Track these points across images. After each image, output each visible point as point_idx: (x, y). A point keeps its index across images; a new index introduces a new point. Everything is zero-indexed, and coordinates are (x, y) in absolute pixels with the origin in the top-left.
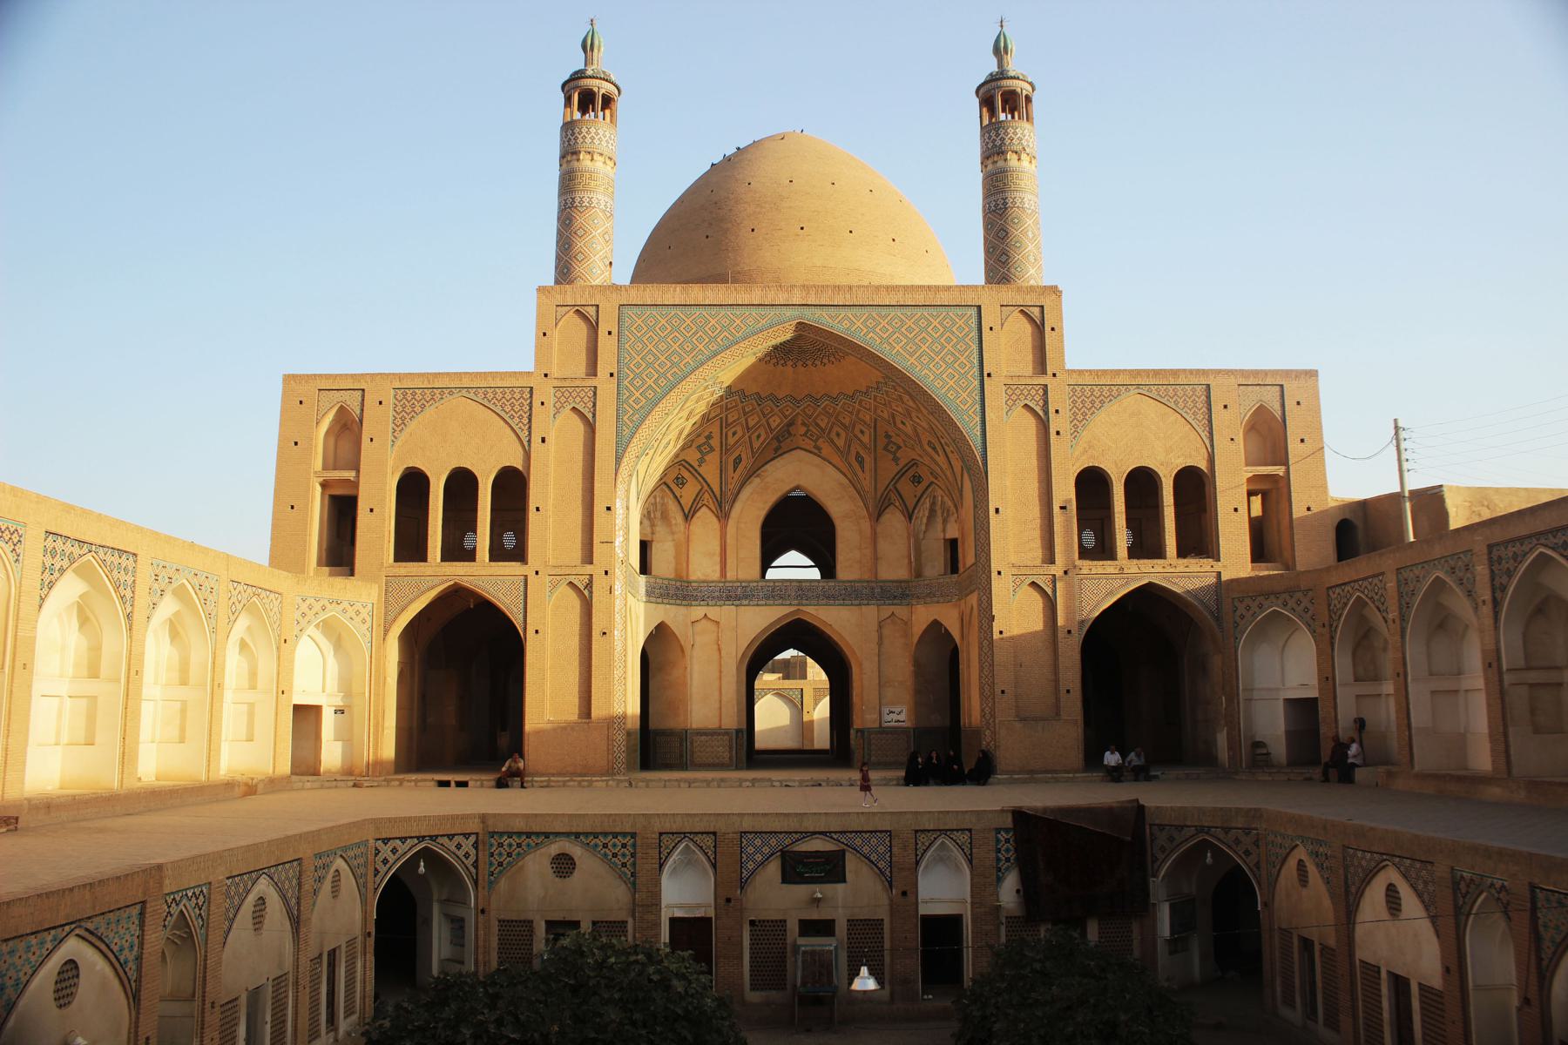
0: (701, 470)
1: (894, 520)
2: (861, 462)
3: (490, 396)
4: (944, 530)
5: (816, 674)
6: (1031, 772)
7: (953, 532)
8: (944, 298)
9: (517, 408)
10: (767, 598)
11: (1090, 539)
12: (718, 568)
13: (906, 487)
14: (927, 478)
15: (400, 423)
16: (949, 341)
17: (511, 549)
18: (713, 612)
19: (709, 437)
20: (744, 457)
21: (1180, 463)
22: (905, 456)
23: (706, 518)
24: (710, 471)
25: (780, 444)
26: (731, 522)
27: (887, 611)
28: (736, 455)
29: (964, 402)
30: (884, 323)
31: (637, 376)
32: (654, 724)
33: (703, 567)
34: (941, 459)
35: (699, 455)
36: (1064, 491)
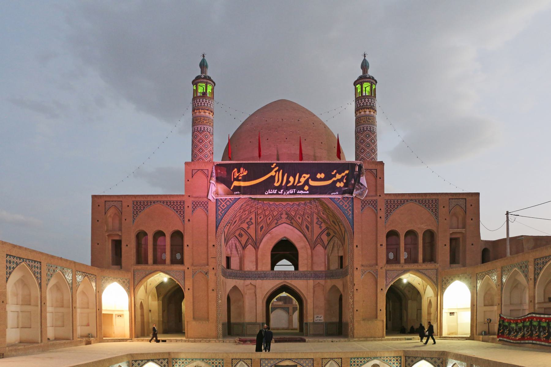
0: (248, 231)
7: (341, 254)
9: (179, 208)
10: (273, 277)
11: (391, 256)
12: (255, 266)
14: (332, 234)
15: (136, 214)
19: (251, 219)
20: (264, 226)
21: (425, 227)
24: (252, 231)
25: (277, 221)
26: (259, 250)
28: (261, 225)
29: (346, 206)
33: (249, 266)
34: (337, 227)
35: (247, 226)
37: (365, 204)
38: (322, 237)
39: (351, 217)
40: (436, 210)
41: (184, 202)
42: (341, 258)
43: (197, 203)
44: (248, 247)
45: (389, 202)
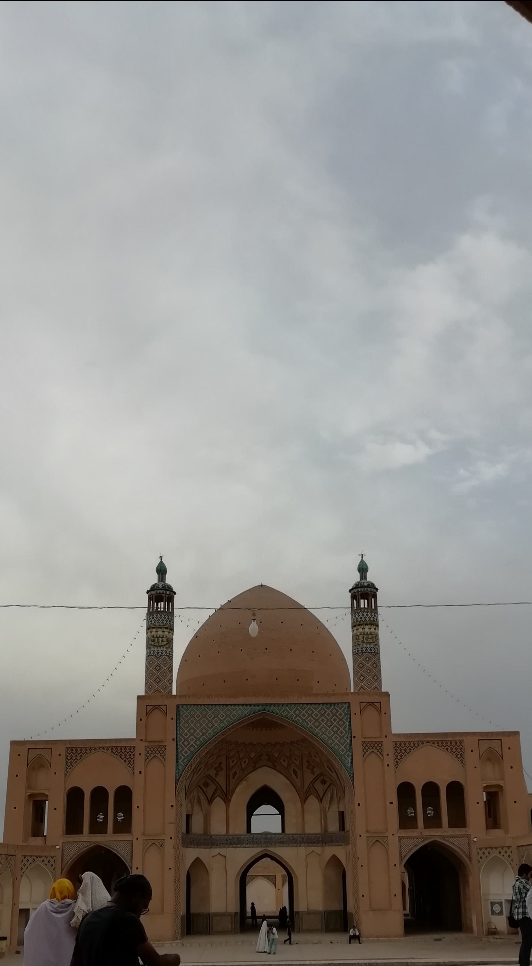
0: (216, 779)
1: (312, 801)
2: (295, 773)
3: (114, 751)
4: (338, 808)
5: (280, 873)
6: (378, 937)
7: (341, 810)
8: (333, 700)
9: (128, 757)
13: (319, 786)
16: (335, 720)
17: (124, 827)
18: (223, 851)
19: (220, 763)
20: (238, 772)
22: (317, 771)
23: (218, 802)
26: (231, 804)
27: (311, 849)
28: (234, 771)
29: (343, 751)
30: (304, 712)
31: (186, 740)
32: (192, 911)
33: (218, 828)
34: (334, 775)
35: (215, 772)
36: (393, 796)
37: (367, 748)
38: (315, 785)
39: (349, 765)
40: (461, 754)
41: (134, 748)
42: (342, 815)
43: (152, 749)
44: (215, 800)
45: (398, 745)
